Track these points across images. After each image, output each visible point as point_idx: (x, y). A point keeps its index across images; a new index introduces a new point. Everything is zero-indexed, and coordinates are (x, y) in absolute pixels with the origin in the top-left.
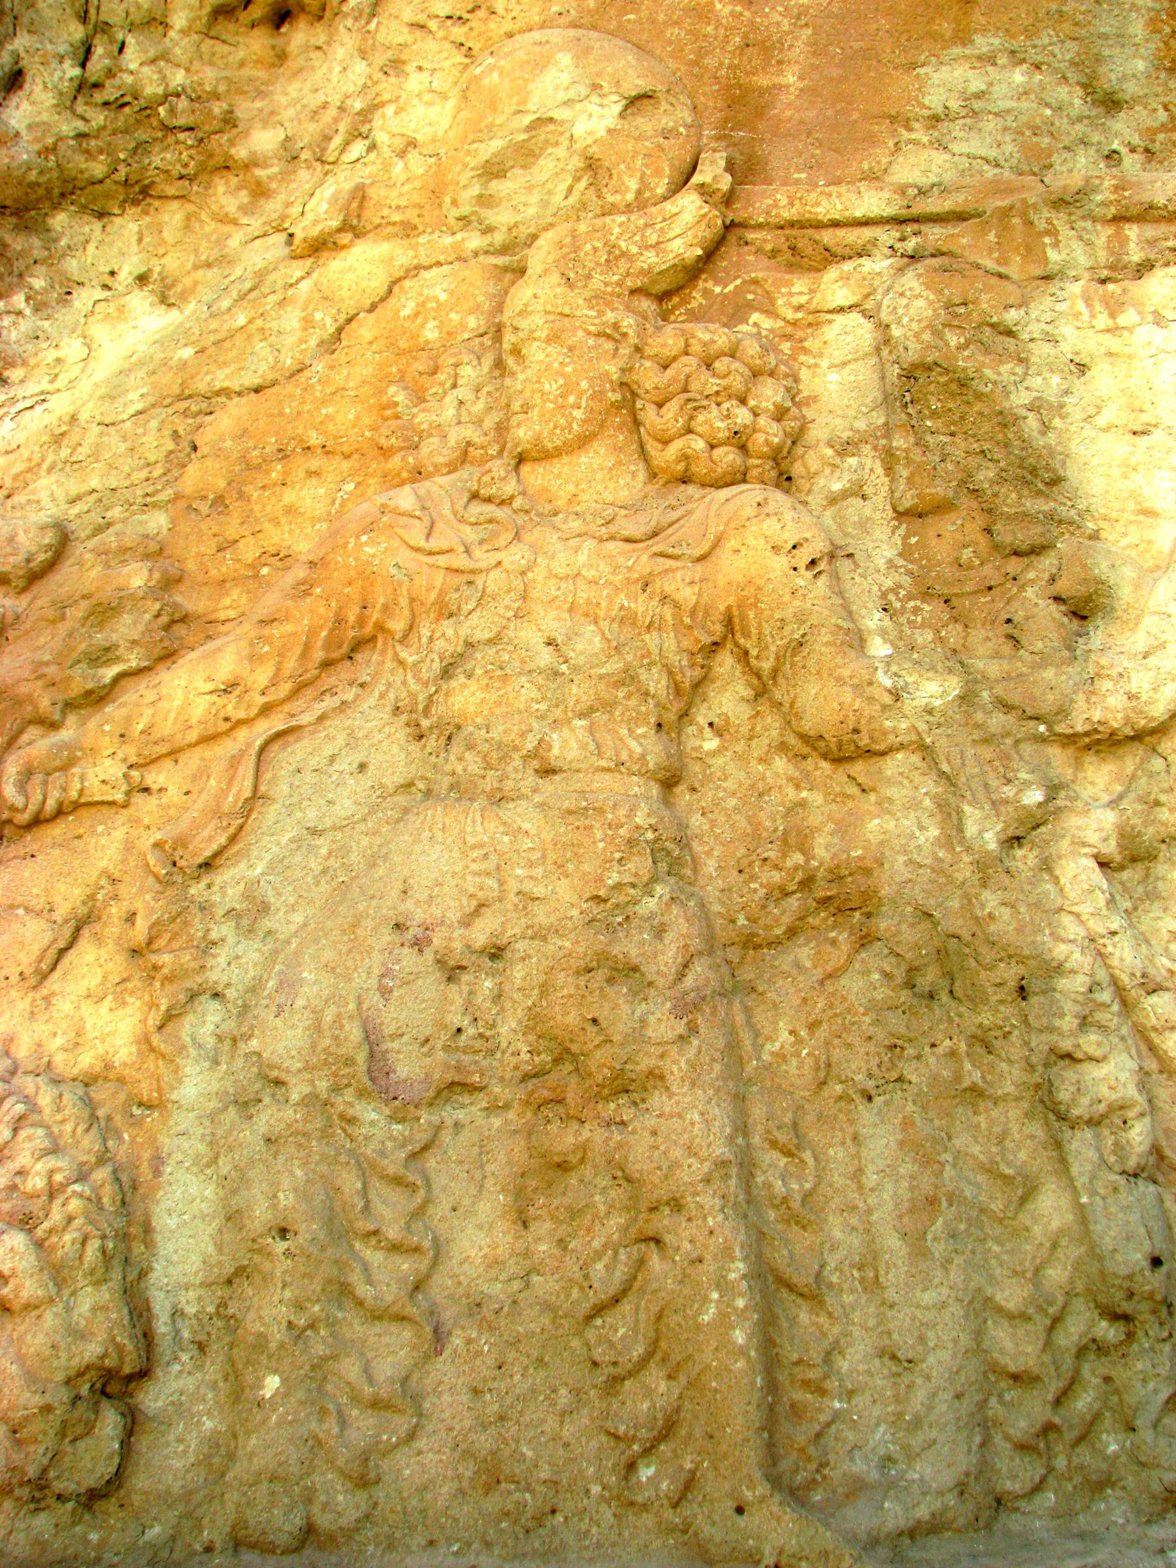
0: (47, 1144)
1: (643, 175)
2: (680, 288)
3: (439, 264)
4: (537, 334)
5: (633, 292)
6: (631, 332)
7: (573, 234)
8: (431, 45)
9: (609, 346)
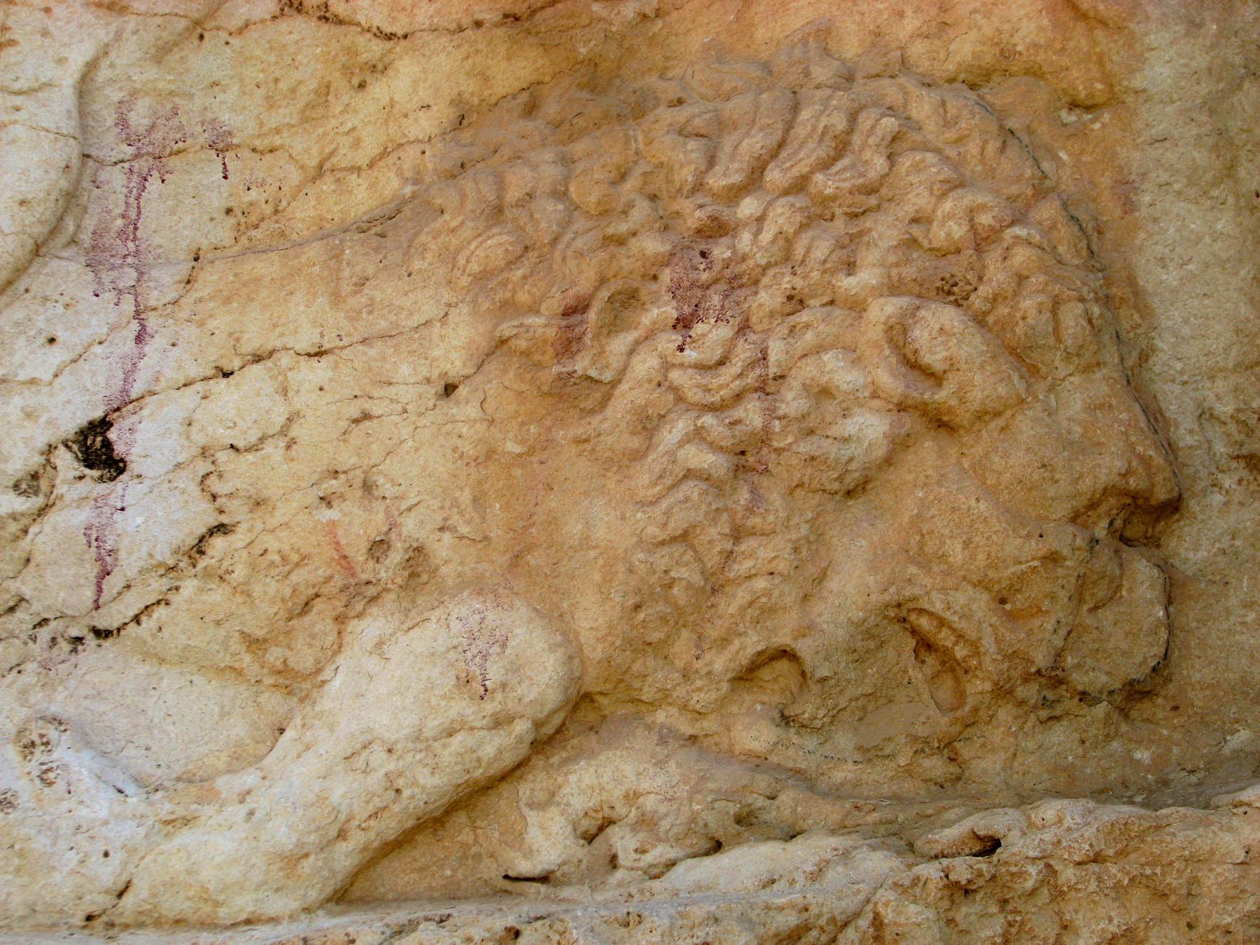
0: (947, 173)
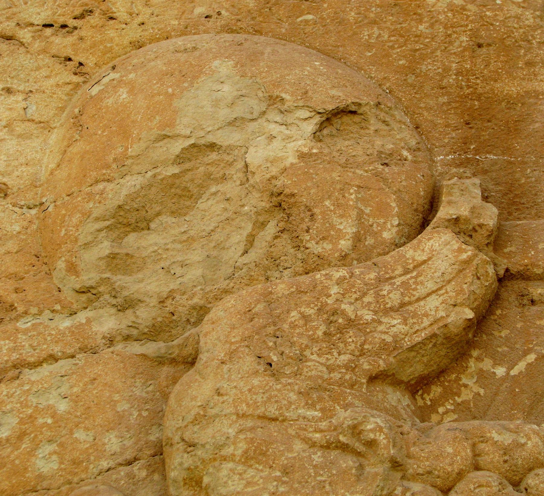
1: (360, 215)
2: (442, 372)
3: (53, 358)
4: (229, 450)
5: (373, 379)
6: (381, 438)
7: (268, 298)
8: (24, 60)
9: (348, 462)
